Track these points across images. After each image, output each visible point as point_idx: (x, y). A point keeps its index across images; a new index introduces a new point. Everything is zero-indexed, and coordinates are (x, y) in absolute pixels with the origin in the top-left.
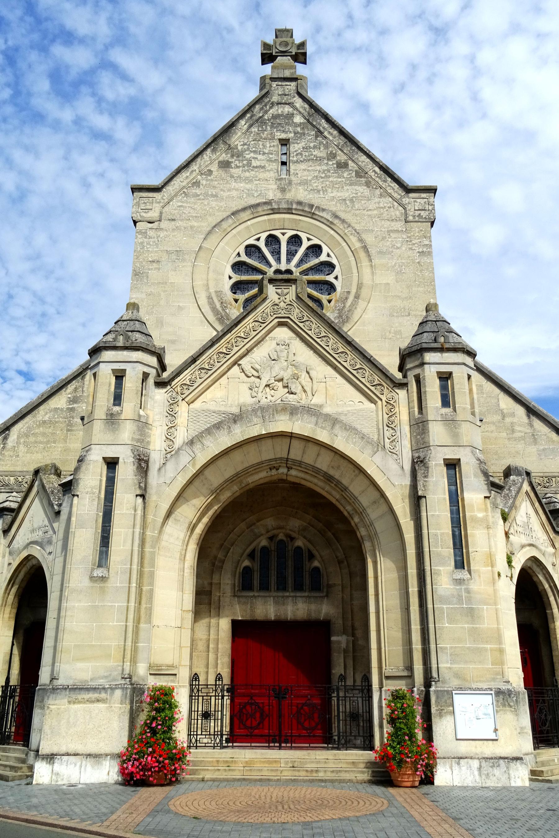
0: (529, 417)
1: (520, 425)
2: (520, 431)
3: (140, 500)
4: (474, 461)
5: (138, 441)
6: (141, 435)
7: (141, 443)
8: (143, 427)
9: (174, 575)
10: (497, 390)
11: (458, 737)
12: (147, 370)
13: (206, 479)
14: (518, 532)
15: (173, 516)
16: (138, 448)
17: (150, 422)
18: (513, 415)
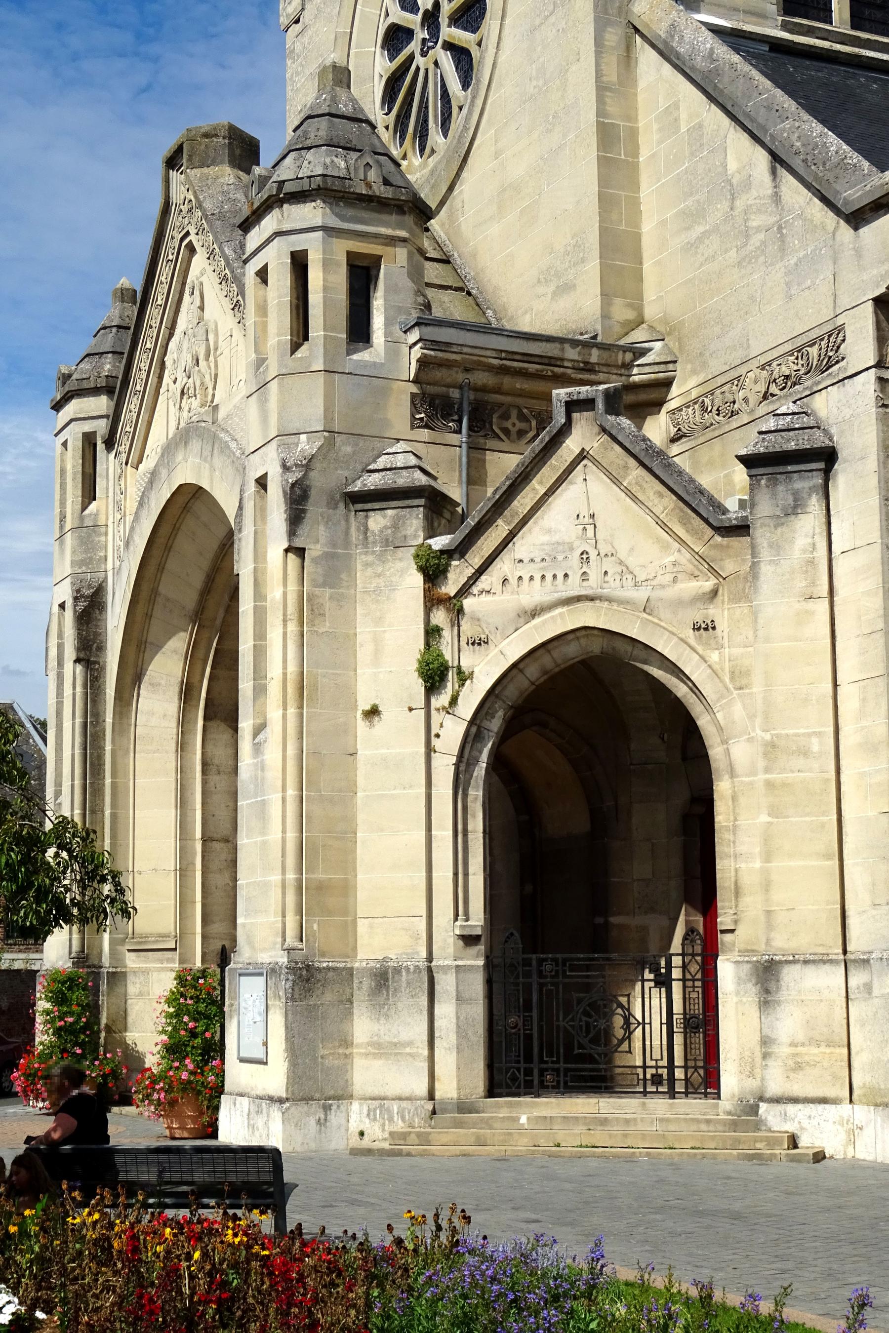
0: (774, 172)
1: (759, 211)
2: (758, 229)
3: (79, 668)
4: (279, 470)
5: (82, 563)
6: (86, 551)
7: (87, 565)
8: (89, 536)
9: (168, 782)
10: (726, 121)
11: (242, 1055)
12: (88, 427)
13: (168, 600)
14: (513, 581)
15: (146, 679)
16: (82, 576)
17: (102, 521)
18: (747, 184)
